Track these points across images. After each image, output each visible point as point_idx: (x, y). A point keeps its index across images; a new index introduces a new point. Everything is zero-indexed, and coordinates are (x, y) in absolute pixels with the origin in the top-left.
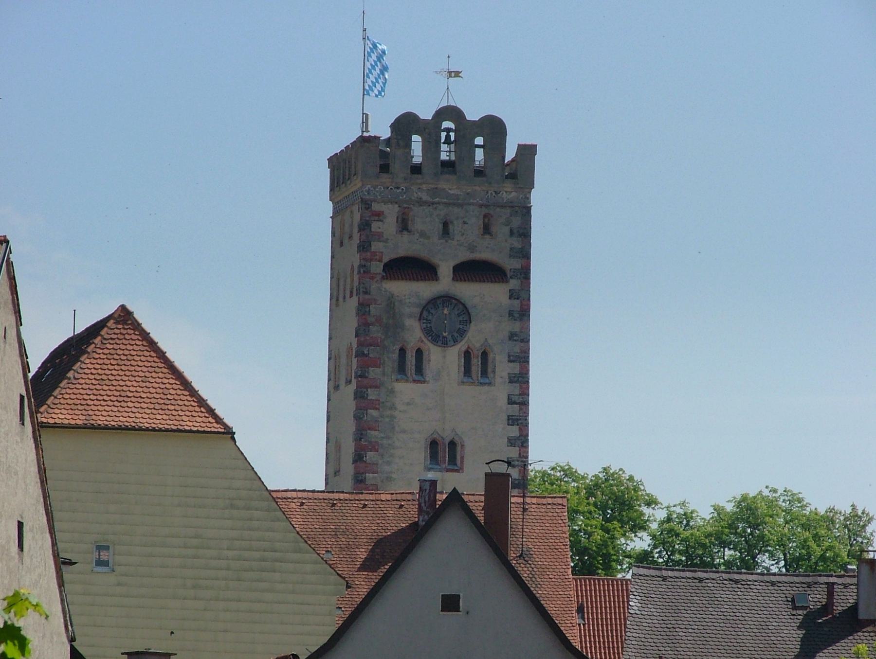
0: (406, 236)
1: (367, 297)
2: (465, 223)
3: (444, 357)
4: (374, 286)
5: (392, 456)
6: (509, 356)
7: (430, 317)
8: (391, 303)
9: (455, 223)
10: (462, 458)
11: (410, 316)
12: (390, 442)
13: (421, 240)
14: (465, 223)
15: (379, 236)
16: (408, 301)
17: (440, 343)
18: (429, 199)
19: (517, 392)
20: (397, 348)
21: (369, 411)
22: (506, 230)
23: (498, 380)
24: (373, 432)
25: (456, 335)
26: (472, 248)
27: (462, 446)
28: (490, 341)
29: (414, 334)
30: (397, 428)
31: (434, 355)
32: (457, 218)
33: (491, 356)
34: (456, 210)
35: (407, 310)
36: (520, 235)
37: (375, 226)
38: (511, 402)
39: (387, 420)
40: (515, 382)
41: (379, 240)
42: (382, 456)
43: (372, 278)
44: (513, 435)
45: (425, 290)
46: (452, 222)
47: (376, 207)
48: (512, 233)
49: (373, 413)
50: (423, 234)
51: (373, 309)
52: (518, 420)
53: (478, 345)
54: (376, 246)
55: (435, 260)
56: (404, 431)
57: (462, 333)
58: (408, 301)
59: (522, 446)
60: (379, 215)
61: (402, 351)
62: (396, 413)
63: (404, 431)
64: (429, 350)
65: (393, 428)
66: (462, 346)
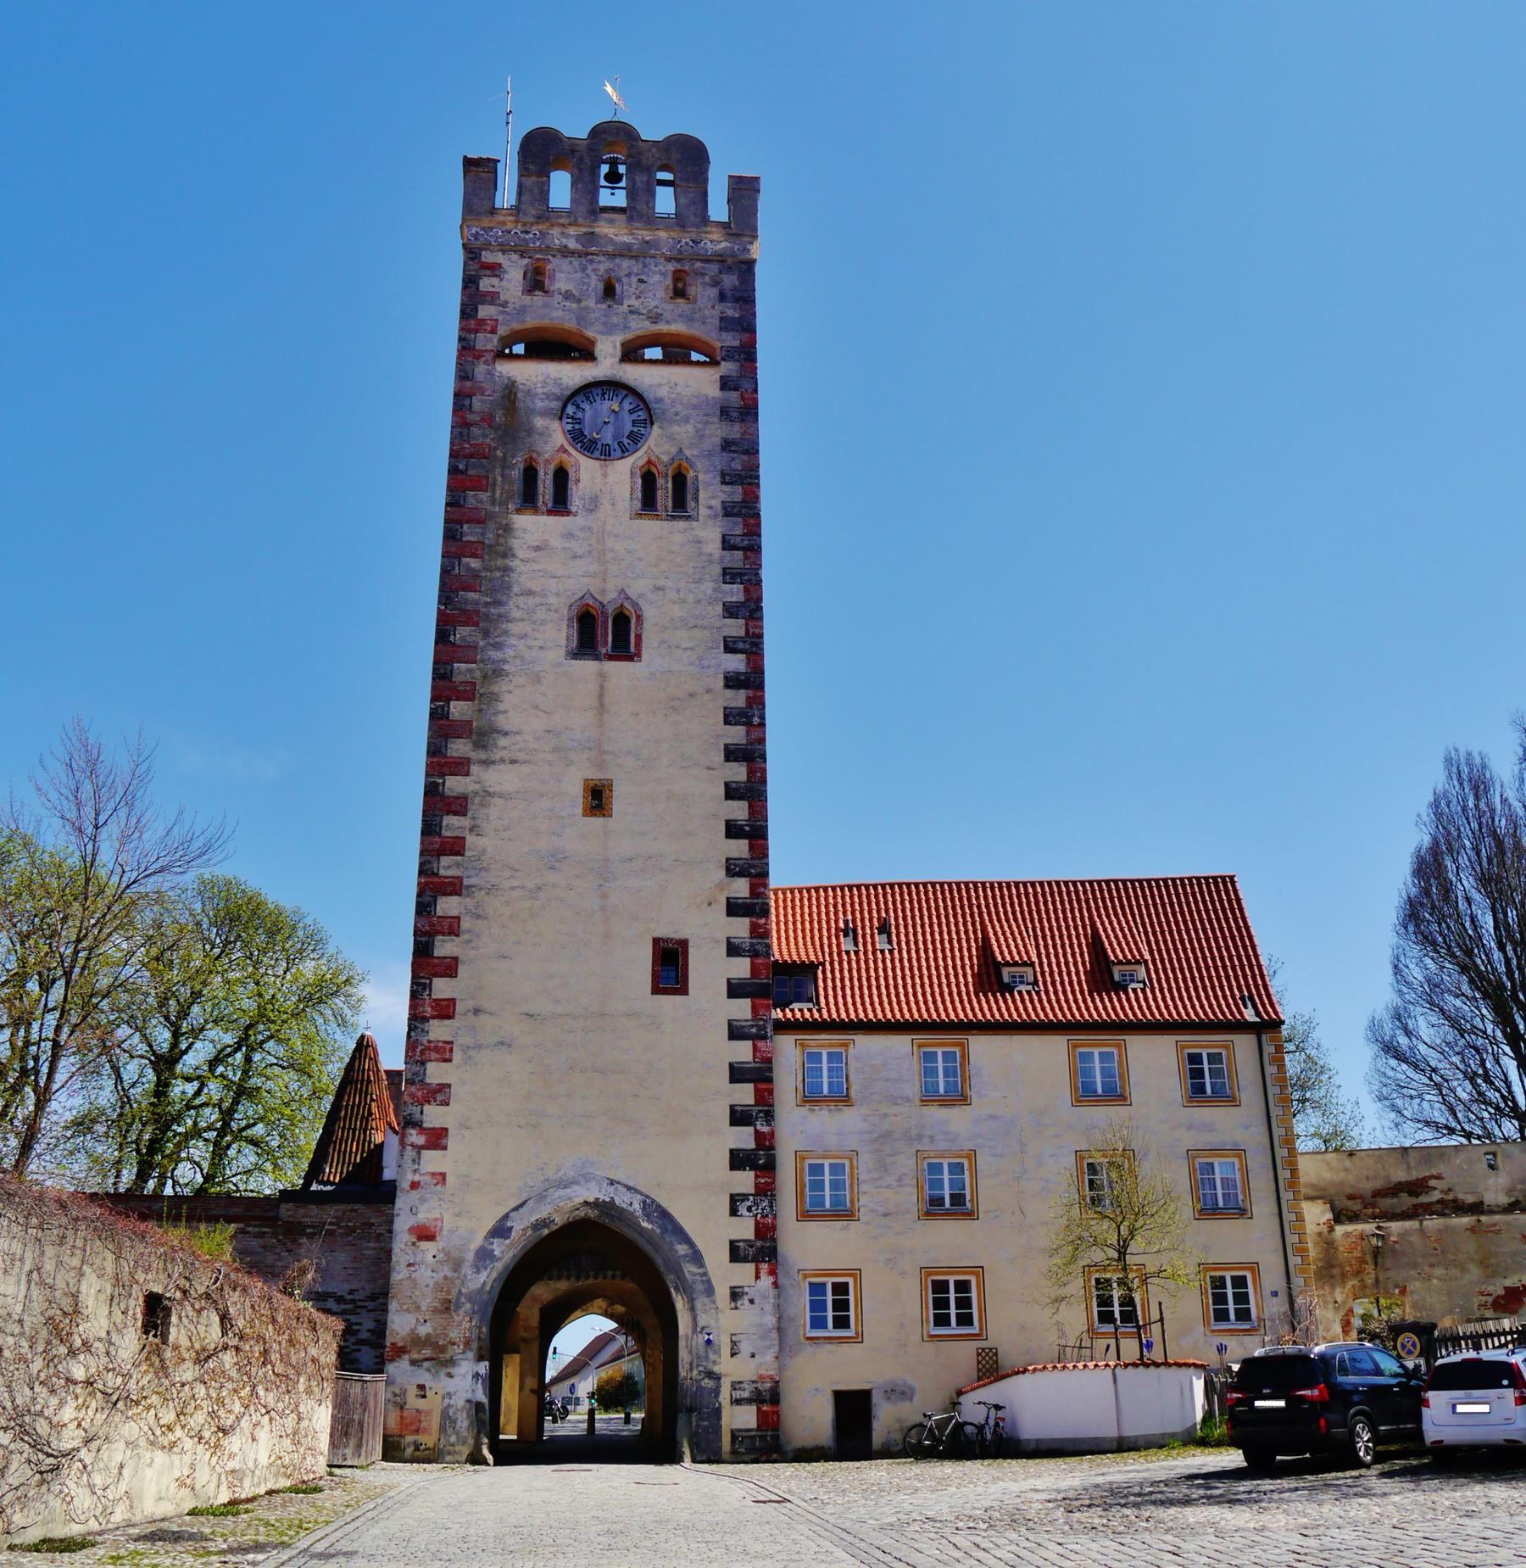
0: (538, 298)
1: (469, 384)
2: (641, 281)
3: (605, 475)
4: (480, 370)
5: (505, 633)
6: (723, 475)
7: (580, 415)
8: (510, 392)
9: (625, 280)
10: (639, 637)
11: (546, 413)
12: (502, 610)
13: (567, 303)
14: (641, 281)
15: (492, 298)
16: (540, 391)
17: (597, 454)
18: (579, 247)
19: (738, 530)
20: (519, 461)
21: (465, 560)
22: (713, 292)
23: (703, 511)
24: (472, 595)
25: (626, 441)
26: (655, 318)
27: (639, 617)
28: (687, 453)
29: (552, 439)
30: (516, 589)
31: (587, 472)
32: (629, 275)
33: (691, 474)
34: (626, 263)
35: (539, 404)
36: (737, 300)
37: (486, 284)
38: (727, 544)
39: (498, 574)
40: (734, 515)
41: (492, 303)
42: (486, 634)
43: (478, 357)
44: (734, 599)
45: (571, 374)
46: (619, 280)
47: (487, 257)
48: (722, 297)
49: (474, 563)
50: (568, 296)
51: (477, 403)
52: (741, 575)
53: (665, 458)
54: (484, 311)
55: (590, 333)
56: (530, 593)
57: (636, 439)
58: (540, 391)
59: (751, 618)
60: (495, 269)
61: (530, 474)
62: (515, 563)
63: (530, 593)
64: (577, 466)
65: (509, 587)
66: (638, 458)
